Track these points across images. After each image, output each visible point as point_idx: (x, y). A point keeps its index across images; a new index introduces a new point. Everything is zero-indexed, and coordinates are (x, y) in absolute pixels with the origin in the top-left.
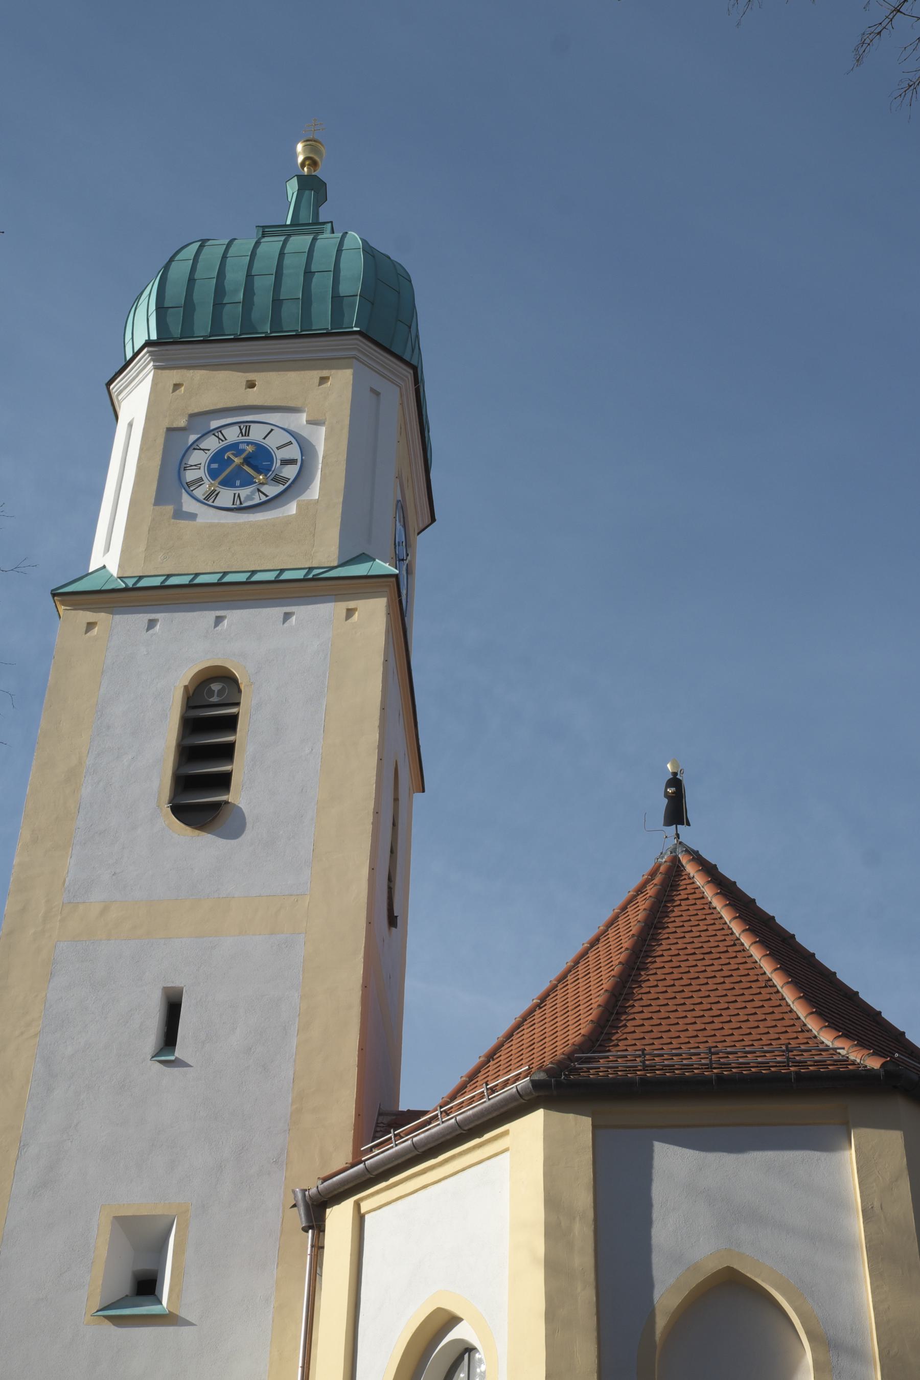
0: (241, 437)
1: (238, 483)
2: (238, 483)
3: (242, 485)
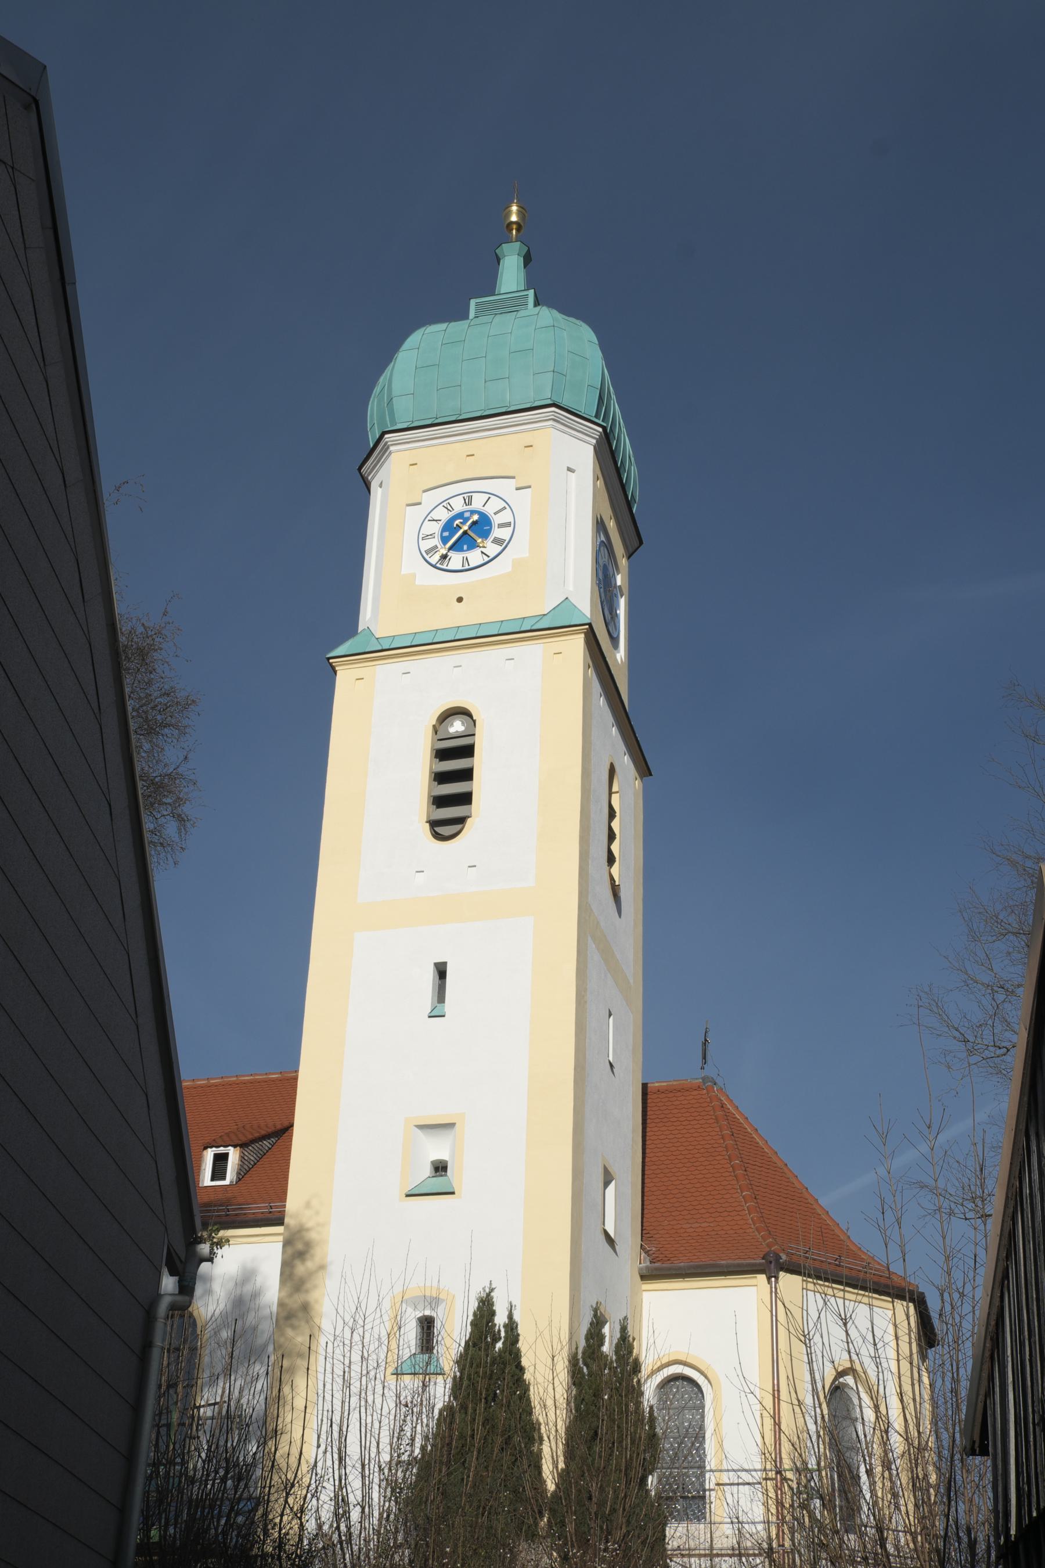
0: (465, 507)
1: (465, 547)
2: (465, 547)
3: (469, 549)
